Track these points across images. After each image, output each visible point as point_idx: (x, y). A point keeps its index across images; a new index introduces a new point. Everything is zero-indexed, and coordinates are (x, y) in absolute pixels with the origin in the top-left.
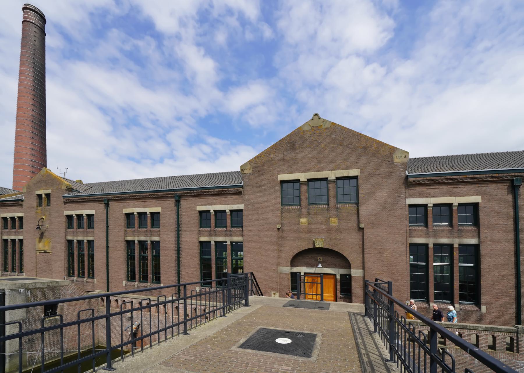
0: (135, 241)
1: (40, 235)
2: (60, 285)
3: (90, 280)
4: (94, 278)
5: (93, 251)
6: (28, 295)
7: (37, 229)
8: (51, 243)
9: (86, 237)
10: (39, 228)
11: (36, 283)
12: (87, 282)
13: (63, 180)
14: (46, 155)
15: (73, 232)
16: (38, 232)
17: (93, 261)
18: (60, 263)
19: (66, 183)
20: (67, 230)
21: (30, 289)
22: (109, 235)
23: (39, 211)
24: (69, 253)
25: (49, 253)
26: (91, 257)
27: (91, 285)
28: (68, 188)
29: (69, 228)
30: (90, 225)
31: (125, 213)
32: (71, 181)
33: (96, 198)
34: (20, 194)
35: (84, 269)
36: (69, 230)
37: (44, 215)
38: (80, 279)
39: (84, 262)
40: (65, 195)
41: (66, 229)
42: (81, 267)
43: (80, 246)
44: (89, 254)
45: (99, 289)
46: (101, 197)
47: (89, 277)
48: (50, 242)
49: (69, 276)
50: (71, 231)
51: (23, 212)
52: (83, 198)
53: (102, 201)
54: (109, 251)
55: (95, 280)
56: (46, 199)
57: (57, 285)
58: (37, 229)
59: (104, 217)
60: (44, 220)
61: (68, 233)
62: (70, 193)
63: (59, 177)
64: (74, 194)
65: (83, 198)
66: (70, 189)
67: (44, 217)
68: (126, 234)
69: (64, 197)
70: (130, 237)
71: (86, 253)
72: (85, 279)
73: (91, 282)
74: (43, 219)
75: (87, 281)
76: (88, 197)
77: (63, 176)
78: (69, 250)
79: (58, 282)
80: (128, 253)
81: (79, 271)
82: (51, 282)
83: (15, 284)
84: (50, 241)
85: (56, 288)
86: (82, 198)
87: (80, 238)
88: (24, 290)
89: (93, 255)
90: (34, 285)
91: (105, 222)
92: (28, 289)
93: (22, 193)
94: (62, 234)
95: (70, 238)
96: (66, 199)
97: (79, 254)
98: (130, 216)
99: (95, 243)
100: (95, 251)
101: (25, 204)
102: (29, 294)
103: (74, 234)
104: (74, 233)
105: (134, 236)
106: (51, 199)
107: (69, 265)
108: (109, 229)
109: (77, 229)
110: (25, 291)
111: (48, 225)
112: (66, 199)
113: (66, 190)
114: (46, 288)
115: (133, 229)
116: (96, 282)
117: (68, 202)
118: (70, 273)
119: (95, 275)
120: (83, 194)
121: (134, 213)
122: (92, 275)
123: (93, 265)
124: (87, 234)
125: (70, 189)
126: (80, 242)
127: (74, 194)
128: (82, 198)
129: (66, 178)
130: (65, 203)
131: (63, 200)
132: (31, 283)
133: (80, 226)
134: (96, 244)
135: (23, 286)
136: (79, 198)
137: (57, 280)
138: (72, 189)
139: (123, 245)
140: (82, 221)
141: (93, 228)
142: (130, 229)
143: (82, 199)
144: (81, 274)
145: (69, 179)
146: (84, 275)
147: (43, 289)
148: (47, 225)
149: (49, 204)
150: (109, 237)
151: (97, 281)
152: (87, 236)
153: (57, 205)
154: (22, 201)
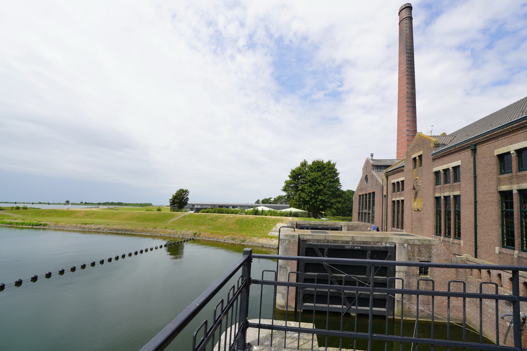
0: (512, 190)
1: (415, 195)
2: (431, 243)
3: (456, 241)
4: (460, 239)
5: (459, 208)
6: (409, 250)
7: (413, 189)
8: (422, 202)
9: (452, 192)
10: (414, 189)
11: (414, 239)
12: (453, 243)
13: (431, 138)
14: (416, 121)
15: (441, 187)
16: (414, 191)
17: (459, 219)
18: (429, 221)
19: (434, 139)
20: (435, 187)
21: (410, 245)
22: (477, 187)
23: (414, 173)
24: (437, 211)
25: (421, 211)
26: (458, 214)
27: (457, 246)
28: (436, 144)
29: (437, 185)
30: (457, 179)
31: (497, 155)
32: (438, 136)
33: (462, 147)
34: (402, 161)
35: (450, 229)
36: (437, 187)
37: (418, 176)
38: (447, 239)
39: (450, 220)
40: (433, 152)
41: (434, 186)
42: (447, 226)
43: (447, 202)
44: (455, 211)
45: (466, 253)
46: (467, 143)
47: (455, 238)
48: (422, 200)
49: (437, 235)
50: (438, 188)
51: (404, 176)
52: (449, 150)
53: (468, 147)
54: (477, 207)
55: (462, 241)
56: (419, 161)
57: (429, 243)
58: (413, 189)
59: (471, 165)
60: (418, 180)
61: (436, 190)
62: (437, 148)
63: (428, 136)
64: (441, 149)
65: (449, 150)
66: (437, 145)
67: (417, 178)
68: (499, 182)
69: (433, 155)
70: (505, 186)
71: (452, 210)
72: (452, 239)
73: (457, 244)
74: (417, 179)
75: (453, 242)
76: (454, 148)
77: (429, 134)
78: (437, 208)
79: (430, 240)
80: (502, 208)
81: (445, 230)
82: (424, 240)
83: (402, 239)
84: (421, 200)
85: (428, 246)
86: (448, 151)
87: (446, 194)
88: (407, 245)
89: (459, 212)
90: (413, 241)
91: (472, 171)
92: (409, 245)
93: (403, 160)
94: (431, 192)
95: (437, 195)
96: (434, 156)
97: (445, 211)
98: (504, 158)
99: (461, 197)
100: (461, 207)
101: (405, 169)
102: (410, 249)
103: (442, 190)
104: (441, 189)
105: (511, 183)
106: (423, 159)
107: (437, 223)
108: (477, 179)
109: (444, 184)
110: (407, 246)
111: (420, 185)
112: (434, 156)
113: (434, 147)
114: (421, 245)
115: (510, 175)
116: (462, 245)
117: (436, 158)
118: (438, 232)
119: (462, 236)
120: (449, 146)
121: (510, 152)
122: (458, 235)
123: (459, 223)
124: (453, 188)
125: (437, 144)
126: (446, 198)
127: (441, 149)
128: (448, 151)
129: (433, 135)
130: (434, 160)
131: (432, 157)
132: (411, 240)
133: (446, 181)
134: (463, 199)
135: (406, 241)
136: (445, 151)
137: (430, 239)
138: (439, 144)
139: (496, 198)
140: (448, 175)
141: (460, 181)
142: (505, 176)
143: (448, 152)
144: (448, 234)
145: (436, 135)
146: (450, 235)
147: (419, 245)
148: (420, 185)
149: (421, 165)
150: (477, 189)
151: (464, 243)
152: (453, 191)
153: (427, 163)
154: (403, 166)
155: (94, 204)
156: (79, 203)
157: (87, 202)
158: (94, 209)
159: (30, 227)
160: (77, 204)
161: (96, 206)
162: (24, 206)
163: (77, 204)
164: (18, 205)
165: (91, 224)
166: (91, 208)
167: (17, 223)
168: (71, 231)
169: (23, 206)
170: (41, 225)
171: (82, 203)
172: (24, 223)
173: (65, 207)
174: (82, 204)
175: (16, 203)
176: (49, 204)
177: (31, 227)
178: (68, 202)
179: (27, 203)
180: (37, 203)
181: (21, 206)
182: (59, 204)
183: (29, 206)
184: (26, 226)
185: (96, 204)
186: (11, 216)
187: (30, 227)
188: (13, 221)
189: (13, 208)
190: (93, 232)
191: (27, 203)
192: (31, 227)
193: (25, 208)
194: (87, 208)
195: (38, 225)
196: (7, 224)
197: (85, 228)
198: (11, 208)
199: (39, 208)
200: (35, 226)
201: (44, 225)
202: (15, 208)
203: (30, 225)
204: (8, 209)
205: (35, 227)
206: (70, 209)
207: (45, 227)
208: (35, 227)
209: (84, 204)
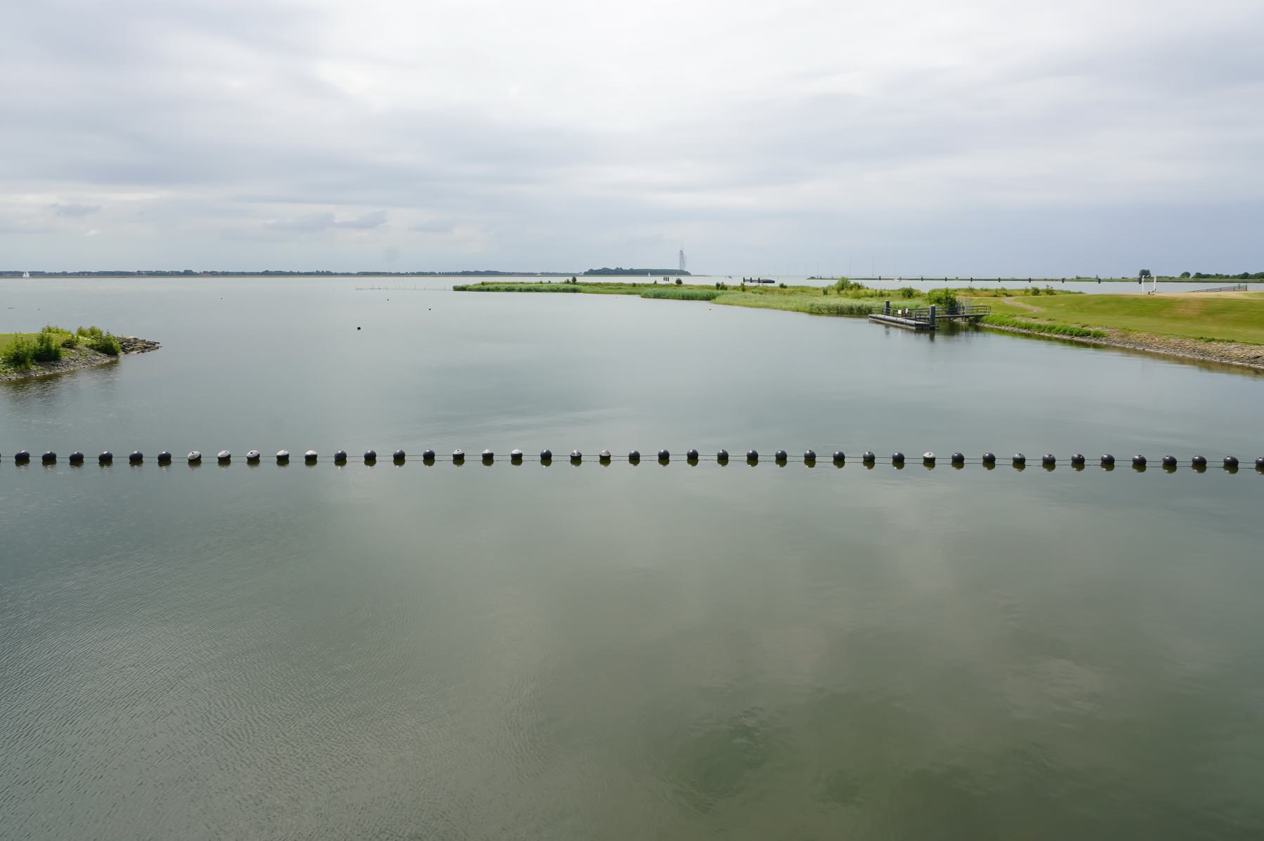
155: (1227, 277)
156: (1178, 275)
157: (1203, 273)
158: (1231, 293)
159: (1065, 337)
160: (1172, 280)
161: (1237, 284)
162: (1048, 286)
163: (1172, 280)
164: (1034, 284)
165: (1228, 341)
166: (1220, 290)
167: (1039, 327)
168: (1164, 357)
169: (1045, 288)
170: (1088, 334)
171: (1188, 274)
172: (1054, 328)
173: (1143, 290)
174: (1186, 279)
175: (1030, 280)
176: (1100, 281)
177: (1069, 338)
178: (1145, 275)
179: (1052, 280)
180: (1072, 280)
181: (1041, 286)
182: (1124, 280)
183: (1057, 286)
184: (1057, 336)
185: (1235, 277)
186: (1026, 310)
187: (1065, 337)
188: (1032, 321)
189: (1027, 291)
190: (1238, 366)
191: (1052, 280)
192: (1069, 338)
193: (1050, 292)
194: (1207, 291)
195: (1082, 336)
196: (1022, 328)
197: (1209, 354)
198: (1023, 292)
199: (1080, 293)
200: (1076, 336)
201: (1097, 335)
202: (1030, 293)
203: (1064, 333)
204: (1018, 293)
205: (1076, 339)
206: (1157, 295)
207: (1098, 342)
208: (1076, 339)
209: (1195, 277)
